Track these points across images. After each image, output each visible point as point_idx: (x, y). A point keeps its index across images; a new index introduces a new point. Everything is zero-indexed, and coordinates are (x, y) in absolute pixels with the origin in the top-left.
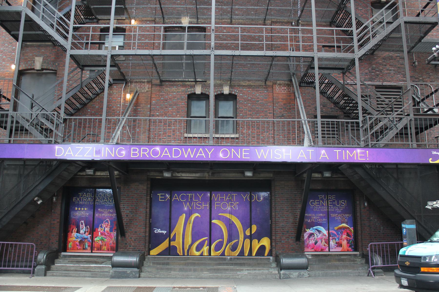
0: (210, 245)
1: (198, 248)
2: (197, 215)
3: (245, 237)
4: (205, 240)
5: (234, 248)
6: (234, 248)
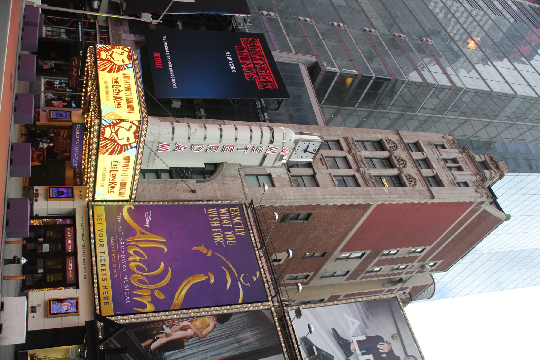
0: (140, 261)
1: (135, 252)
2: (166, 250)
3: (152, 291)
4: (145, 257)
5: (141, 281)
6: (141, 281)
